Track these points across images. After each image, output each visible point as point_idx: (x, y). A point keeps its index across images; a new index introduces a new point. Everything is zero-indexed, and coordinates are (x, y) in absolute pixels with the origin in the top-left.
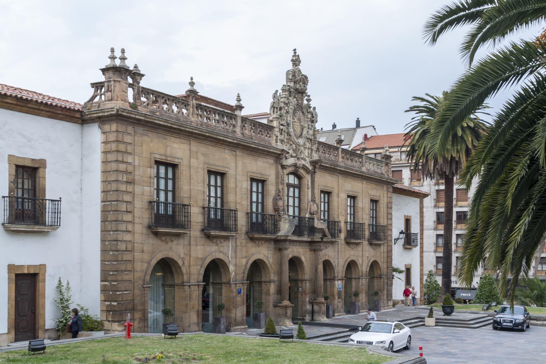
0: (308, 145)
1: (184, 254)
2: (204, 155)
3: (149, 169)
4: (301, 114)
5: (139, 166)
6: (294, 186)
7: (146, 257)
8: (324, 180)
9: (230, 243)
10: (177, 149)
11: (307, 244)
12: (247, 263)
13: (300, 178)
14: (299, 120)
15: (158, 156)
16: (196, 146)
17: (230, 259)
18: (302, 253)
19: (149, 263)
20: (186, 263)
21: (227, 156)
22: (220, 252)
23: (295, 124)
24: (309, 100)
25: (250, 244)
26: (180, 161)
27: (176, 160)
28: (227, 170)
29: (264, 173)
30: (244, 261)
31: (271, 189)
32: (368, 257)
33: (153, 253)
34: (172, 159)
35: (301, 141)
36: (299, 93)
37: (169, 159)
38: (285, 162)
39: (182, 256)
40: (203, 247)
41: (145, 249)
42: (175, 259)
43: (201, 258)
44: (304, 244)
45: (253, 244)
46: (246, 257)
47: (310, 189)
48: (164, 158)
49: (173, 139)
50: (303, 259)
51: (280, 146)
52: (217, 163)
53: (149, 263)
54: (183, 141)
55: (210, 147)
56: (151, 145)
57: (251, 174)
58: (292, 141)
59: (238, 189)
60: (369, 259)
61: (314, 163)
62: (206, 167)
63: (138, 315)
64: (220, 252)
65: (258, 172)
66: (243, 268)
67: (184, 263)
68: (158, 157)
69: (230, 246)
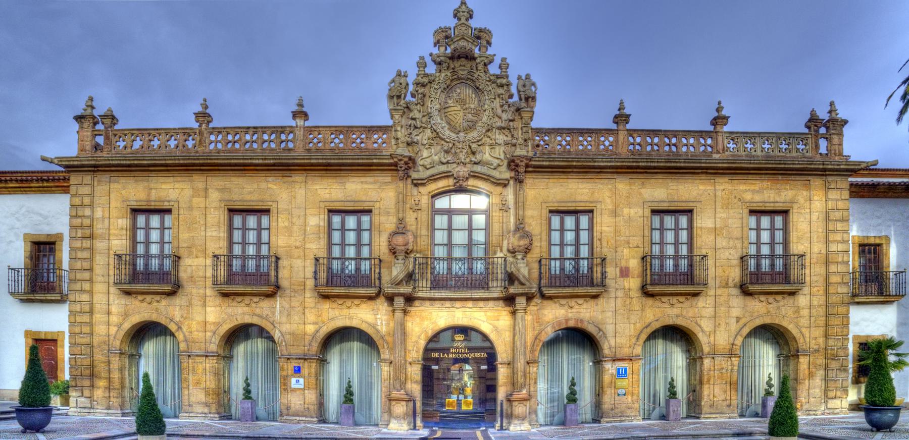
0: (501, 138)
1: (182, 317)
2: (222, 190)
3: (120, 221)
5: (103, 218)
7: (114, 319)
10: (169, 189)
12: (317, 331)
14: (462, 102)
15: (135, 203)
16: (199, 180)
18: (484, 318)
19: (119, 326)
20: (185, 328)
21: (270, 185)
22: (254, 314)
23: (450, 109)
25: (326, 305)
26: (172, 203)
27: (166, 204)
28: (270, 203)
29: (364, 198)
30: (310, 329)
32: (738, 319)
33: (126, 315)
34: (157, 204)
35: (473, 135)
36: (459, 57)
37: (153, 204)
38: (414, 175)
39: (177, 319)
40: (218, 308)
41: (114, 309)
42: (163, 323)
43: (214, 323)
44: (491, 303)
45: (335, 305)
46: (316, 323)
47: (512, 211)
48: (144, 203)
49: (162, 179)
50: (486, 328)
51: (403, 151)
52: (248, 197)
53: (119, 326)
54: (179, 179)
55: (233, 179)
56: (123, 192)
57: (327, 204)
58: (443, 139)
59: (295, 228)
60: (743, 321)
61: (512, 164)
62: (223, 205)
63: (102, 383)
64: (254, 314)
65: (349, 199)
66: (308, 338)
67: (179, 328)
68: (135, 205)
69: (278, 306)
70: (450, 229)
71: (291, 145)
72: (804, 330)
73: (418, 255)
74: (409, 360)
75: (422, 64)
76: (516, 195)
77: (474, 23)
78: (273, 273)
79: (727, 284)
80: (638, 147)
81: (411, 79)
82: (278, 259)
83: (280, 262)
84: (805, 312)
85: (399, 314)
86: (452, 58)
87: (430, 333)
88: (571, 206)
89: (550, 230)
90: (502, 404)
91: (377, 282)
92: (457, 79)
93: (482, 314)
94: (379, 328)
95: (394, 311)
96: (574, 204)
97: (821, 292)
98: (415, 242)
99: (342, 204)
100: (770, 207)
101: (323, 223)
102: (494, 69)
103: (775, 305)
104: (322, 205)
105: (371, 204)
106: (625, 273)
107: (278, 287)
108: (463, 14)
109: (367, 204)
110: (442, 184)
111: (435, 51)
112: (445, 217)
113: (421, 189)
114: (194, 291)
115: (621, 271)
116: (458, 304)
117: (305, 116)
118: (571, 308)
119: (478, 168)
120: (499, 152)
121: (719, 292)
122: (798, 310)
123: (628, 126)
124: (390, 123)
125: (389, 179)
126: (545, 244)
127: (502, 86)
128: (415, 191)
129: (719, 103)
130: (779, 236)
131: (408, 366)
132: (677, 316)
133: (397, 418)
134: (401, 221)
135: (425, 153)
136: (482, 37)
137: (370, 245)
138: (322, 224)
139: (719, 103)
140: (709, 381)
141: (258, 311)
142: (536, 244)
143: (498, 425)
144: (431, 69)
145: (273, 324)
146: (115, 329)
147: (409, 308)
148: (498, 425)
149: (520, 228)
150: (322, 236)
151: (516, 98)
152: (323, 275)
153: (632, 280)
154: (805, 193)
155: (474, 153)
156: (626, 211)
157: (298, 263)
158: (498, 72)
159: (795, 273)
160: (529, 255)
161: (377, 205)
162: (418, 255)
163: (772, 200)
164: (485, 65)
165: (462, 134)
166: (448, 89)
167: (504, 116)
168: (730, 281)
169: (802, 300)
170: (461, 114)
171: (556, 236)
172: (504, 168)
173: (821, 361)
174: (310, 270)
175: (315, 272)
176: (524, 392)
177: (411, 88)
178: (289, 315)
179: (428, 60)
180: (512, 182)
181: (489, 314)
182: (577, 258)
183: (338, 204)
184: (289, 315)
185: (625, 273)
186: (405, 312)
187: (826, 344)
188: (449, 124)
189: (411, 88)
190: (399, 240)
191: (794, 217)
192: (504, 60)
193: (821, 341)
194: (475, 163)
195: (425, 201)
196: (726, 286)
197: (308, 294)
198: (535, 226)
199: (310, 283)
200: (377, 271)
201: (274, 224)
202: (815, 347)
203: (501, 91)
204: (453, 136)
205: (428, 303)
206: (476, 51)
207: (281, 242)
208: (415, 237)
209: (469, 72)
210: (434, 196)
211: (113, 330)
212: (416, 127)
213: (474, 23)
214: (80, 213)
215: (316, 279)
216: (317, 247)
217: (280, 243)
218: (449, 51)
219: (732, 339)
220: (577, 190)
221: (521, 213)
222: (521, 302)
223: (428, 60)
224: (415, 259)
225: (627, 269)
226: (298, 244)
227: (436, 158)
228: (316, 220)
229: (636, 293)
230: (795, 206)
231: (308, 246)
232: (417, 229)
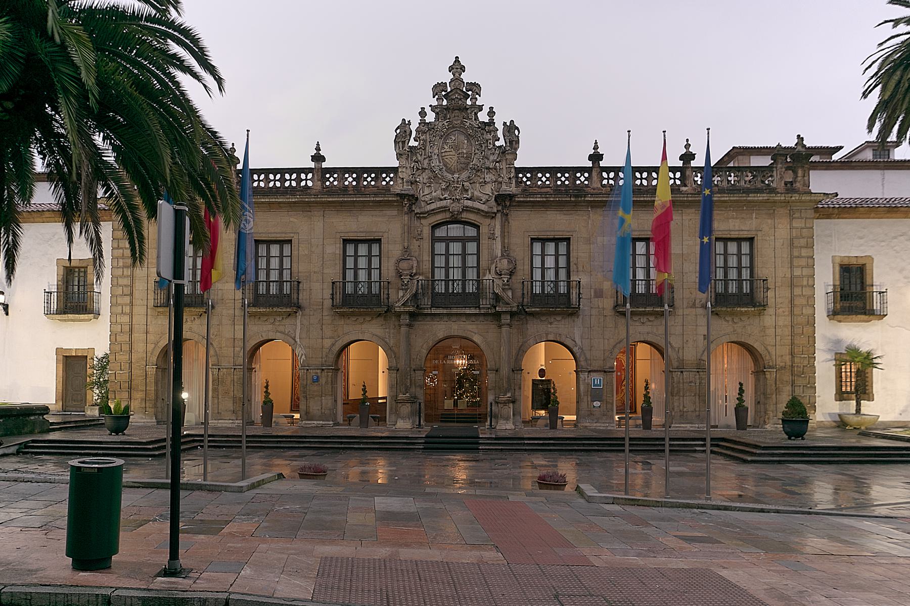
4: (462, 137)
6: (463, 240)
8: (526, 223)
9: (298, 321)
11: (490, 318)
12: (333, 345)
13: (477, 227)
14: (456, 148)
17: (298, 340)
24: (491, 113)
28: (292, 235)
30: (328, 343)
31: (393, 250)
36: (454, 110)
47: (499, 239)
50: (477, 339)
51: (407, 189)
64: (277, 331)
70: (447, 255)
71: (310, 184)
72: (769, 348)
73: (421, 278)
74: (414, 367)
75: (423, 113)
76: (503, 227)
77: (466, 77)
78: (295, 296)
79: (694, 304)
80: (611, 182)
81: (414, 127)
82: (299, 282)
83: (301, 285)
84: (771, 331)
85: (404, 329)
86: (447, 108)
87: (431, 344)
88: (550, 235)
89: (532, 255)
90: (491, 404)
91: (386, 301)
92: (452, 127)
93: (474, 327)
94: (387, 340)
95: (400, 326)
96: (553, 233)
97: (786, 313)
98: (418, 266)
99: (355, 234)
100: (734, 235)
101: (339, 251)
102: (483, 117)
103: (740, 324)
104: (338, 236)
105: (380, 234)
106: (599, 294)
107: (299, 307)
108: (457, 67)
109: (376, 234)
110: (439, 218)
111: (435, 103)
112: (444, 244)
113: (423, 221)
114: (224, 312)
115: (595, 292)
116: (454, 319)
117: (323, 159)
118: (551, 323)
119: (469, 203)
120: (488, 189)
121: (687, 311)
122: (764, 329)
123: (602, 164)
124: (396, 164)
125: (395, 213)
126: (527, 267)
127: (490, 132)
128: (417, 223)
129: (687, 140)
130: (745, 261)
131: (412, 373)
132: (648, 333)
133: (403, 418)
134: (406, 250)
135: (427, 191)
136: (475, 88)
137: (380, 268)
138: (338, 252)
139: (687, 140)
140: (678, 392)
141: (281, 328)
142: (519, 267)
143: (488, 423)
144: (431, 117)
145: (295, 340)
146: (153, 346)
147: (413, 323)
148: (488, 423)
149: (506, 252)
150: (337, 262)
151: (501, 142)
152: (338, 297)
153: (605, 300)
154: (769, 221)
155: (467, 191)
156: (599, 239)
157: (316, 286)
158: (486, 119)
159: (759, 295)
160: (513, 277)
161: (386, 235)
162: (421, 278)
163: (737, 228)
164: (476, 114)
165: (456, 175)
166: (445, 137)
167: (492, 158)
168: (697, 301)
169: (768, 319)
170: (456, 158)
171: (537, 262)
172: (492, 202)
173: (787, 377)
174: (328, 293)
175: (332, 294)
176: (509, 395)
177: (414, 134)
178: (308, 331)
179: (428, 110)
180: (499, 215)
181: (480, 327)
182: (556, 282)
183: (352, 234)
184: (308, 331)
185: (599, 294)
186: (410, 326)
187: (793, 362)
188: (445, 166)
189: (414, 134)
190: (404, 265)
191: (758, 243)
192: (491, 108)
193: (788, 358)
194: (467, 199)
195: (427, 231)
196: (694, 306)
197: (325, 313)
198: (519, 251)
199: (328, 303)
200: (386, 292)
201: (295, 253)
202: (782, 364)
203: (489, 136)
204: (450, 176)
205: (429, 318)
206: (469, 102)
207: (302, 268)
208: (418, 262)
209: (462, 122)
210: (435, 227)
211: (151, 347)
212: (418, 169)
213: (466, 77)
214: (121, 245)
215: (333, 299)
216: (334, 272)
217: (301, 269)
218: (445, 103)
219: (699, 355)
220: (556, 222)
221: (506, 241)
222: (506, 319)
223: (428, 110)
224: (418, 281)
225: (601, 291)
226: (316, 269)
227: (434, 194)
228: (335, 249)
229: (609, 311)
230: (759, 234)
231: (325, 271)
232: (419, 255)
